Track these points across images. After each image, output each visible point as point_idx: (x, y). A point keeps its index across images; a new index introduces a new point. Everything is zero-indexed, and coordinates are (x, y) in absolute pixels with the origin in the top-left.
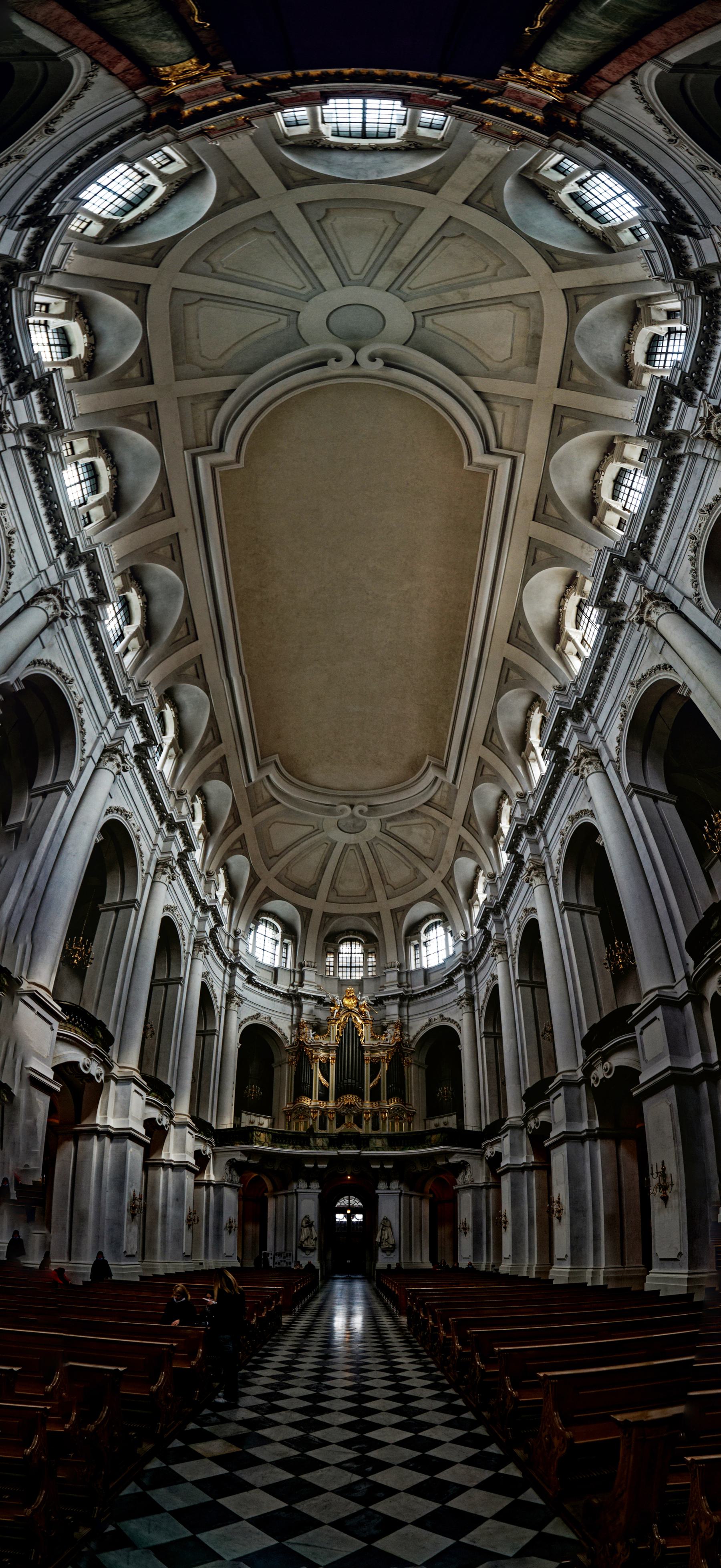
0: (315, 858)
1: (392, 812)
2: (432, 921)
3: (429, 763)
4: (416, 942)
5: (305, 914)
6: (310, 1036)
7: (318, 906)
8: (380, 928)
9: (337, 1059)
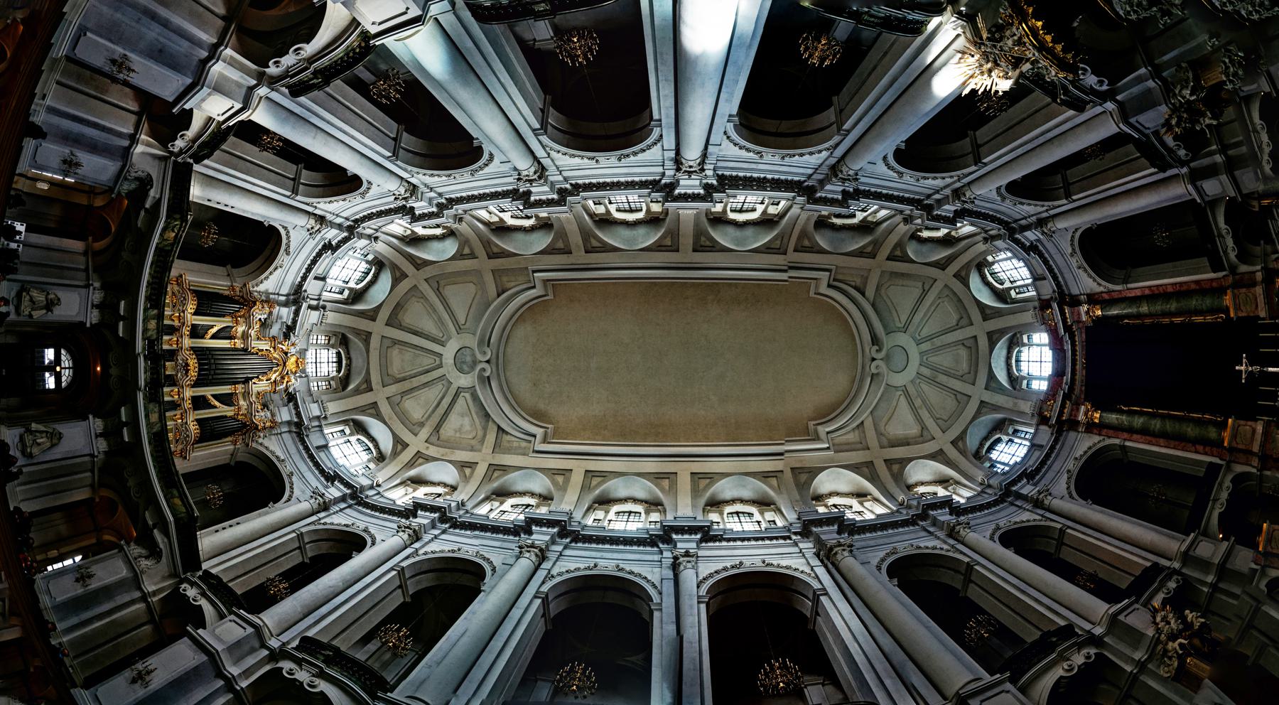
0: (428, 326)
1: (484, 398)
2: (371, 445)
3: (548, 428)
4: (348, 431)
5: (372, 314)
6: (259, 314)
7: (378, 328)
8: (357, 392)
9: (236, 349)
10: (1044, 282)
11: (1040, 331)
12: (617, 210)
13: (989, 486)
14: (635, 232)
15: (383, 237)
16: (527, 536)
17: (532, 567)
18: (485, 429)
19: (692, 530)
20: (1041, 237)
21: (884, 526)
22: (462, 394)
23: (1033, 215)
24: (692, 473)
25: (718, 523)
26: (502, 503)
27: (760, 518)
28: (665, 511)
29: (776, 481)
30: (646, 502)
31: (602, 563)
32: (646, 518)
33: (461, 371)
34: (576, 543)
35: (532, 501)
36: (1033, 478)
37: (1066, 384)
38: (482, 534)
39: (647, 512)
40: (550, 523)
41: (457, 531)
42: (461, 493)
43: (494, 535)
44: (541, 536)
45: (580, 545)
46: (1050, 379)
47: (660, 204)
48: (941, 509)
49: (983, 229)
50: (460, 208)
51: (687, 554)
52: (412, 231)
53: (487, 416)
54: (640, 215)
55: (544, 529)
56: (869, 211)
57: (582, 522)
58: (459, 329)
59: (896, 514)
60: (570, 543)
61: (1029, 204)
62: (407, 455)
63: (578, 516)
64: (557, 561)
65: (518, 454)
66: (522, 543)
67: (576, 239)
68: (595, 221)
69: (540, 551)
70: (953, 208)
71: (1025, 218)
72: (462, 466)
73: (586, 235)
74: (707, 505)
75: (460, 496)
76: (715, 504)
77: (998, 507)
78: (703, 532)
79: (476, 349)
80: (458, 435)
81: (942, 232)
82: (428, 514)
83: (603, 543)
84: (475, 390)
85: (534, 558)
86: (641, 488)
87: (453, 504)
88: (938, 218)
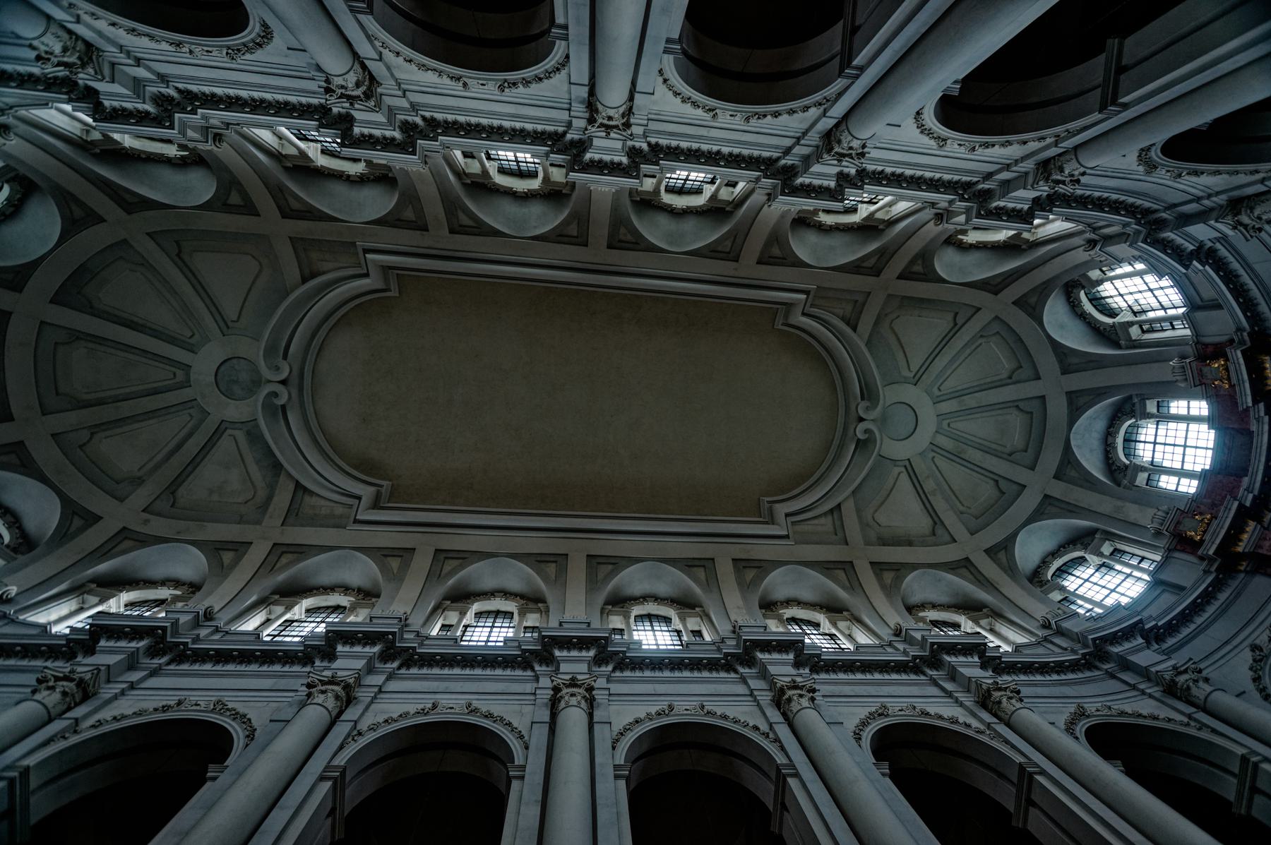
1: (273, 438)
3: (381, 486)
10: (1214, 313)
11: (1188, 396)
12: (499, 171)
13: (1061, 632)
14: (525, 210)
15: (22, 128)
16: (325, 664)
17: (326, 719)
18: (272, 488)
19: (583, 643)
20: (1230, 232)
21: (867, 667)
22: (229, 432)
23: (1218, 193)
24: (588, 556)
25: (622, 630)
26: (289, 608)
27: (680, 627)
28: (547, 611)
29: (703, 574)
30: (522, 596)
31: (444, 700)
32: (520, 622)
33: (229, 395)
34: (408, 668)
35: (344, 600)
36: (1159, 639)
37: (1248, 490)
38: (242, 668)
39: (522, 613)
40: (368, 638)
41: (185, 667)
42: (210, 593)
43: (265, 668)
44: (349, 662)
45: (414, 671)
46: (1203, 476)
47: (564, 170)
48: (965, 655)
49: (1089, 225)
50: (217, 116)
51: (573, 683)
52: (107, 138)
53: (277, 467)
54: (535, 184)
55: (358, 649)
56: (881, 203)
57: (423, 632)
58: (226, 327)
59: (889, 650)
60: (399, 668)
61: (1218, 173)
62: (95, 537)
63: (416, 621)
64: (372, 702)
65: (328, 526)
66: (314, 678)
67: (435, 210)
68: (464, 185)
69: (344, 688)
70: (1031, 194)
71: (1198, 199)
72: (213, 549)
73: (451, 206)
74: (607, 603)
75: (200, 604)
76: (619, 602)
77: (1080, 675)
78: (598, 647)
79: (262, 363)
80: (215, 497)
81: (1002, 235)
82: (123, 644)
83: (451, 666)
84: (257, 426)
85: (331, 703)
86: (517, 576)
87: (184, 619)
88: (999, 214)
